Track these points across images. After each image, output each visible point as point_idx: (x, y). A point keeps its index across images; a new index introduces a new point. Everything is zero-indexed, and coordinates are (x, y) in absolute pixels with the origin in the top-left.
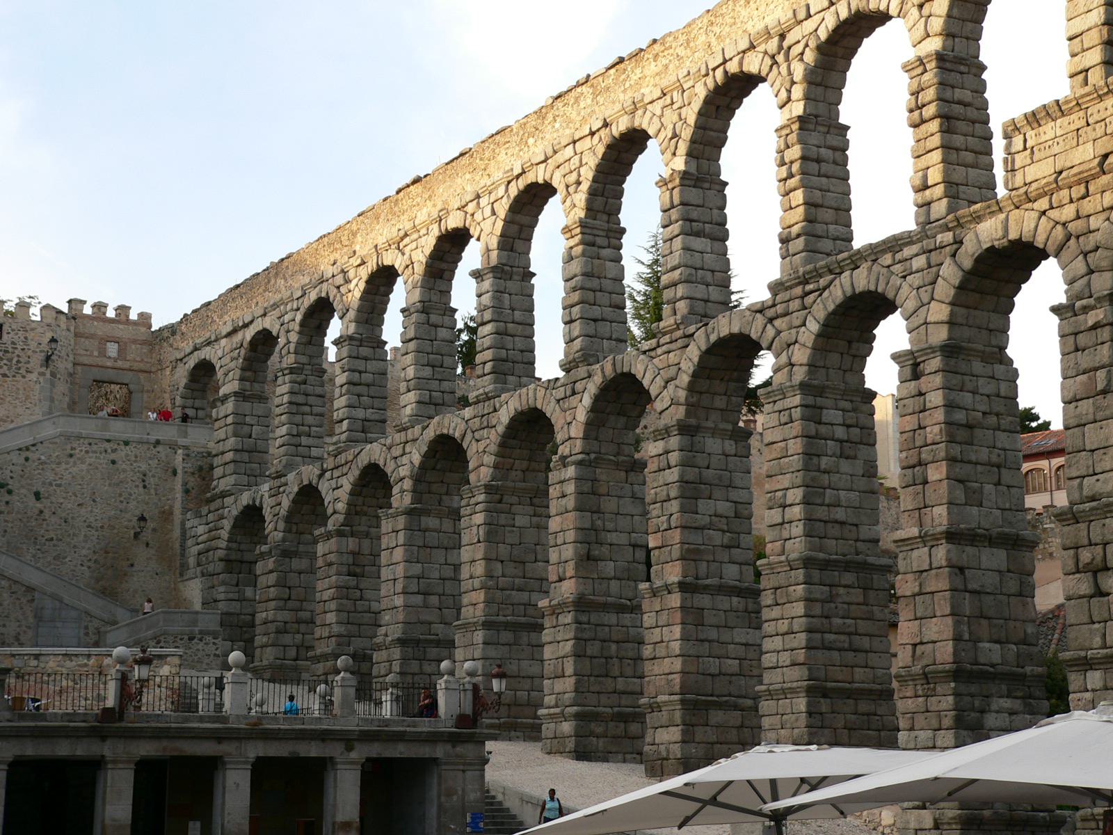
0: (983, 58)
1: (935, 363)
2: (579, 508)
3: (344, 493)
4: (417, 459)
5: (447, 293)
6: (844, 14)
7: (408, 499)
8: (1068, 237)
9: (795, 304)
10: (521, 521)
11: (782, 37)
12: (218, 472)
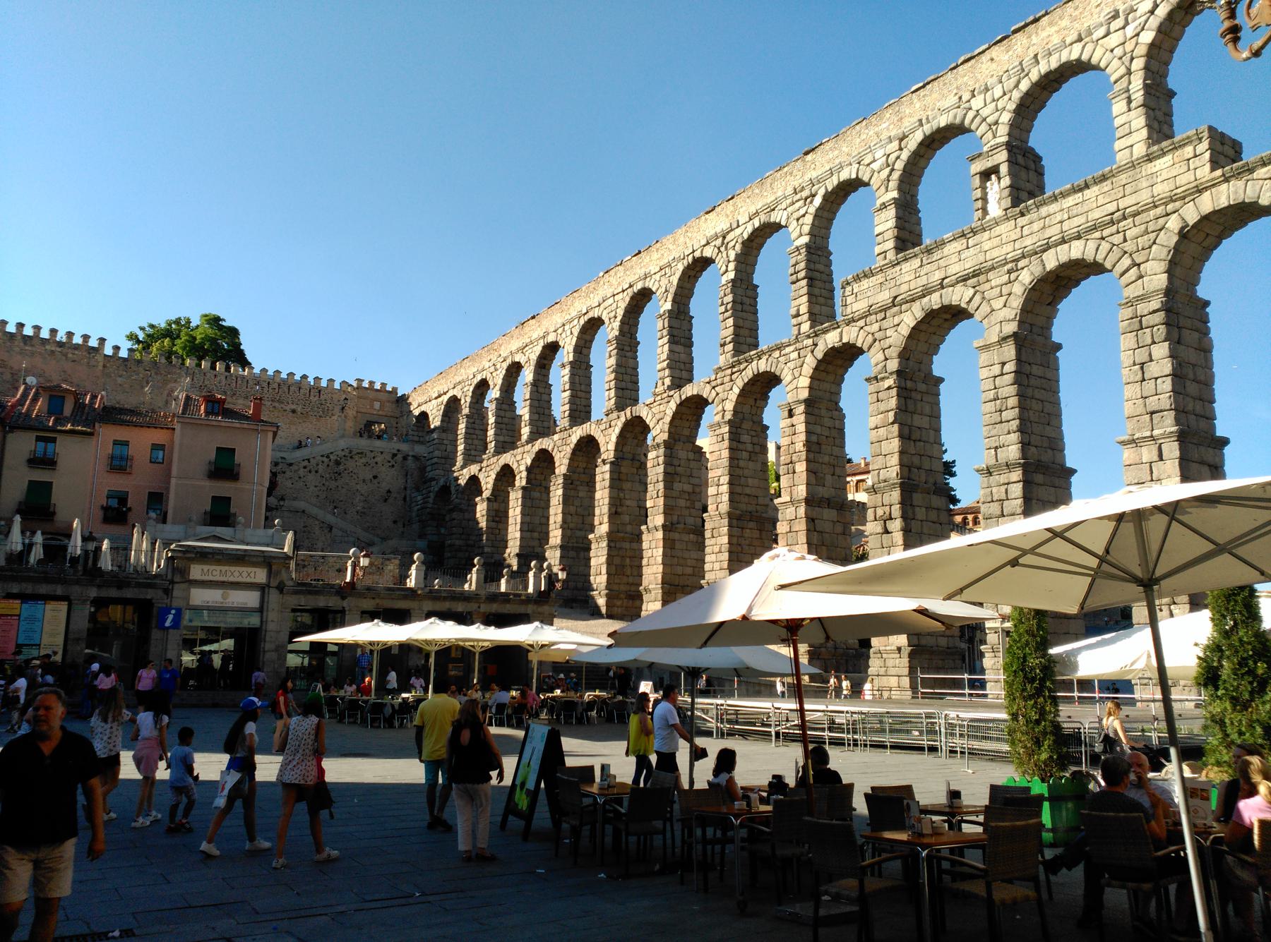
0: (831, 248)
1: (801, 408)
2: (611, 487)
3: (491, 480)
4: (529, 462)
5: (547, 376)
6: (757, 225)
7: (524, 483)
8: (875, 341)
9: (727, 379)
10: (581, 494)
11: (724, 238)
12: (429, 468)
